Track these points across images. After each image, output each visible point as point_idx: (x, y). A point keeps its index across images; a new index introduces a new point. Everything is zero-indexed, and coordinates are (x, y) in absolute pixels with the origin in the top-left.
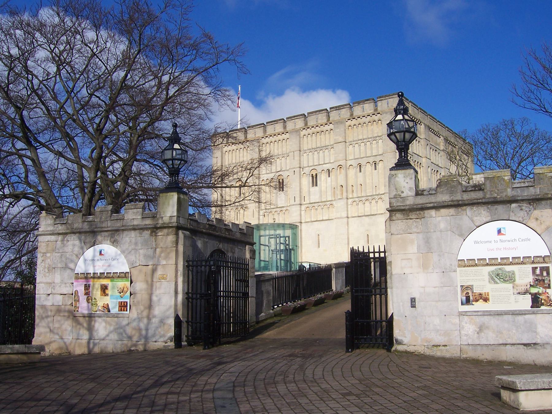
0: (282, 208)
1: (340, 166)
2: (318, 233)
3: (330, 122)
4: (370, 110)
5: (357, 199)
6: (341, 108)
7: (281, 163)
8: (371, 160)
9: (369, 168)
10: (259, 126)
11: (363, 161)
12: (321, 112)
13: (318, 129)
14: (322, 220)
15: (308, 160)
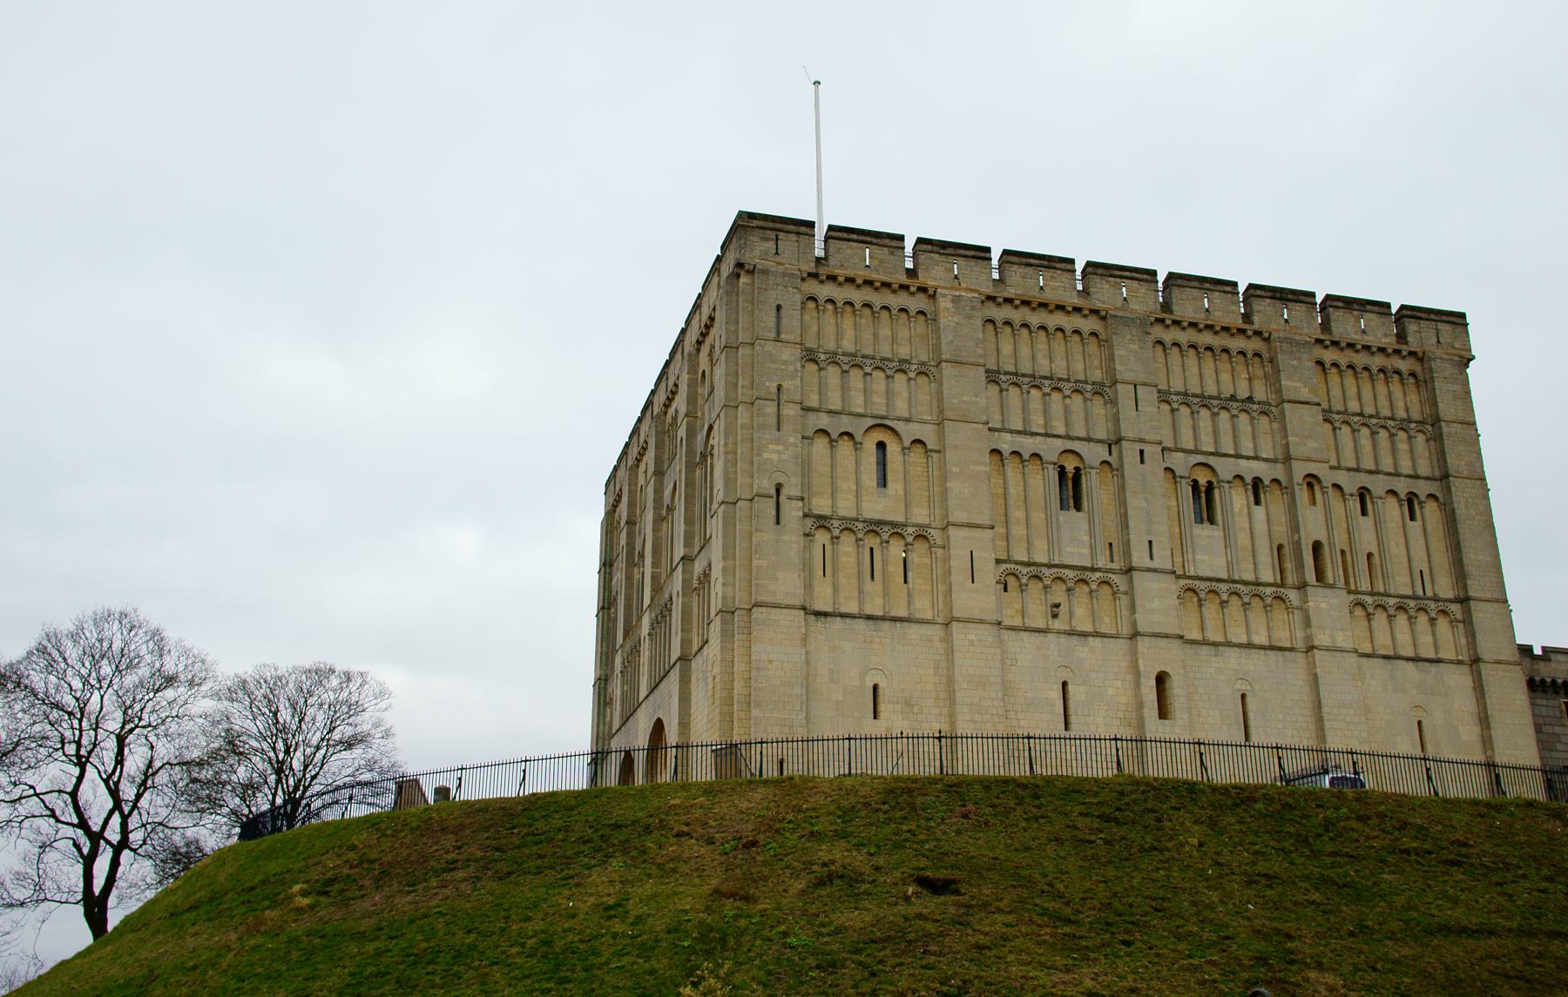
0: (1090, 574)
1: (1312, 481)
2: (1244, 687)
3: (1256, 327)
4: (1386, 335)
5: (1369, 600)
6: (1290, 296)
7: (1067, 409)
8: (1402, 487)
9: (1392, 511)
10: (972, 253)
11: (1378, 485)
12: (1219, 288)
13: (1207, 338)
14: (1250, 646)
15: (1203, 431)
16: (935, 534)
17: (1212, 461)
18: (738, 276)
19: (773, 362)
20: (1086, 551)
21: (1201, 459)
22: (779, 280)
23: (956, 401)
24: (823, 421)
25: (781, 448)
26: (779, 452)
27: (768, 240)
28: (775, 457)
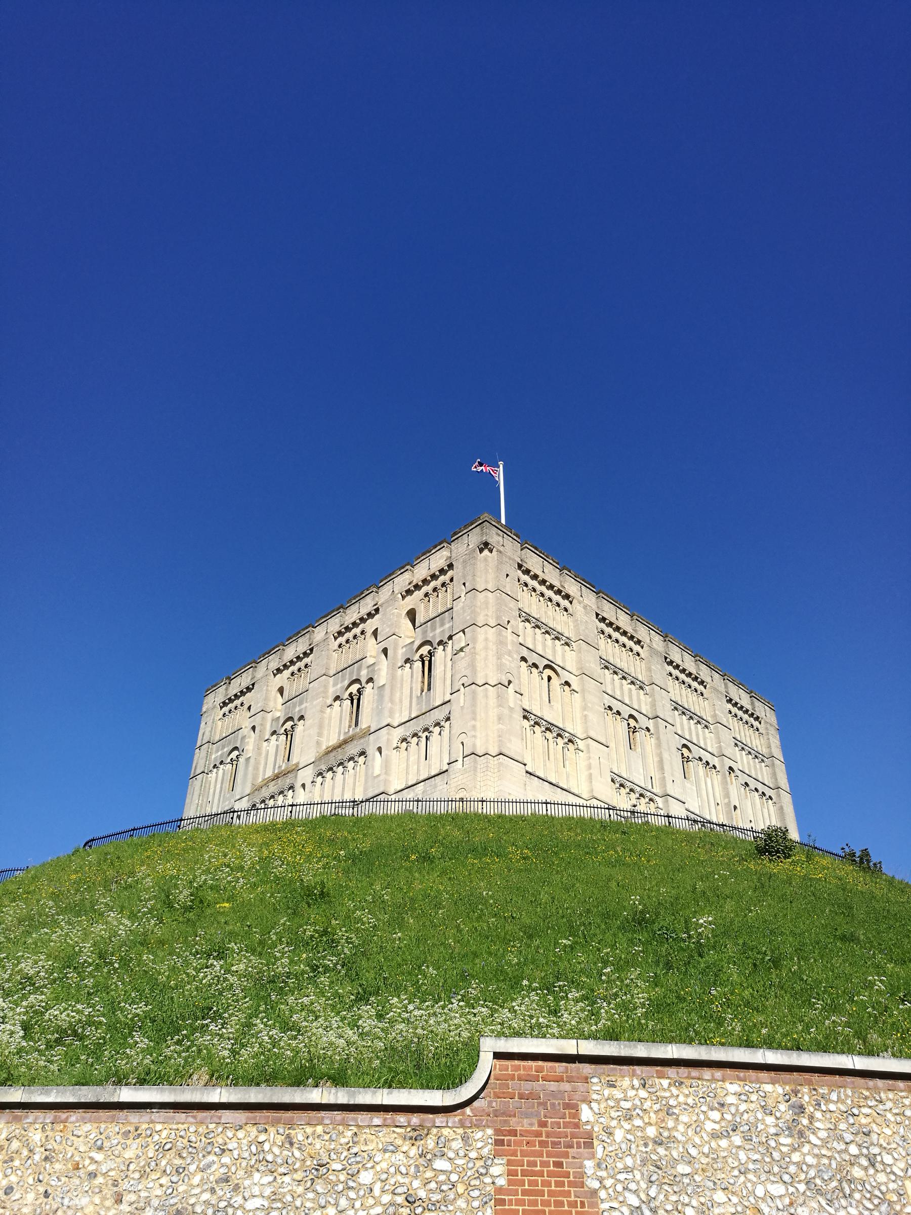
7: (630, 690)
16: (581, 744)
17: (689, 744)
18: (481, 551)
19: (506, 606)
20: (642, 778)
21: (685, 742)
22: (507, 560)
23: (587, 665)
24: (525, 653)
25: (510, 659)
26: (509, 661)
27: (499, 535)
28: (508, 663)
